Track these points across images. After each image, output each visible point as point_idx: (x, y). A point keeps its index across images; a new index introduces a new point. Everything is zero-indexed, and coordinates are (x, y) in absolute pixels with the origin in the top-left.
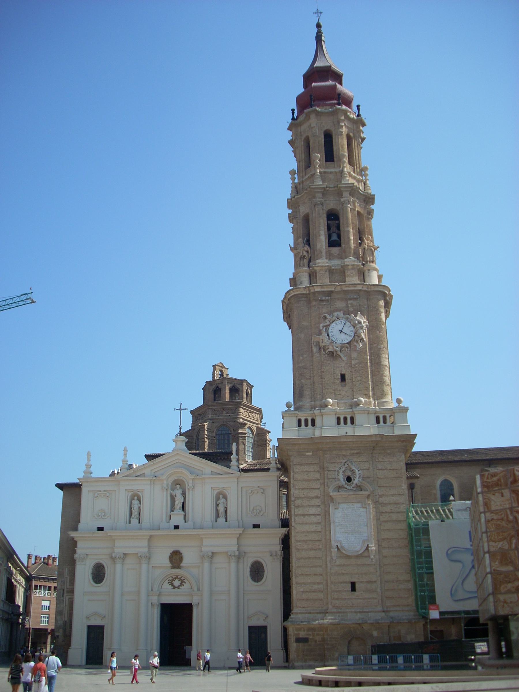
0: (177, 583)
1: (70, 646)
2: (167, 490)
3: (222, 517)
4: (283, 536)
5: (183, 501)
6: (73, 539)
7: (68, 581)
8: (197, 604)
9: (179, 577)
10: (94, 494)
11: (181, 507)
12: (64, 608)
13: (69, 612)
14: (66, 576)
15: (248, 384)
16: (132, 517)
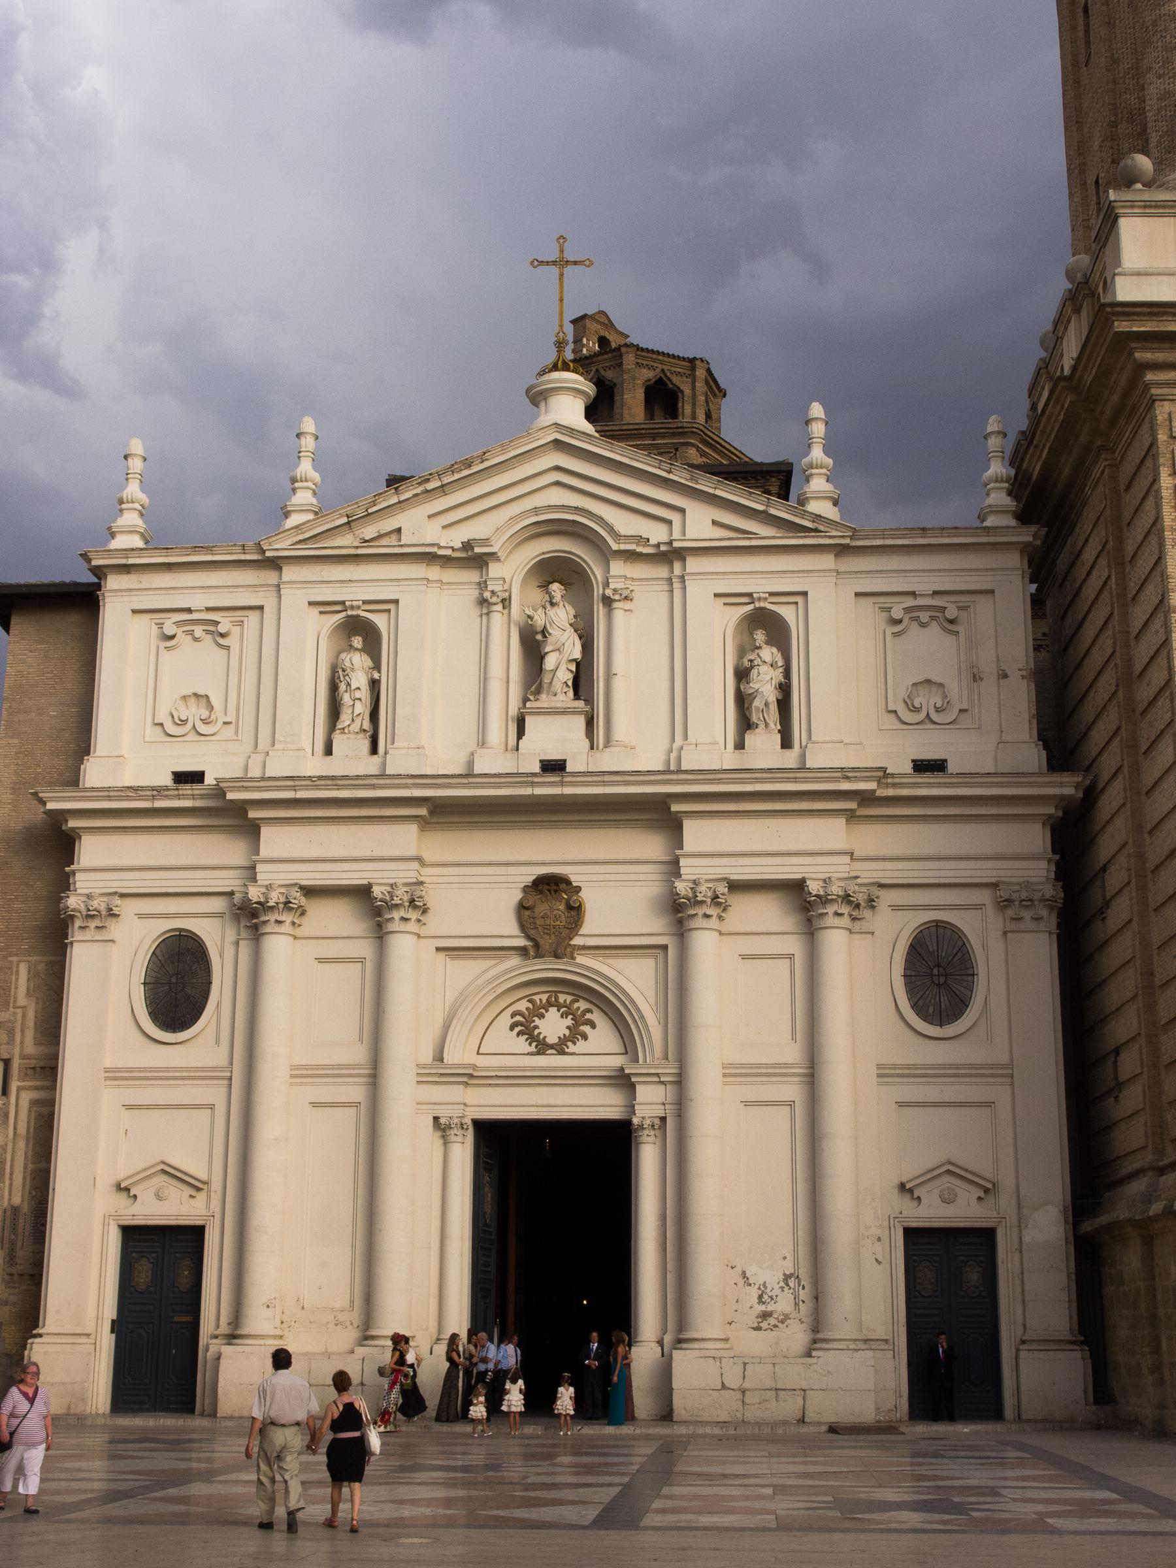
0: (553, 1026)
1: (36, 1326)
2: (506, 602)
3: (767, 725)
4: (1060, 814)
5: (577, 654)
6: (59, 817)
7: (30, 1023)
8: (657, 1122)
9: (562, 998)
10: (160, 626)
11: (570, 683)
12: (10, 1146)
13: (30, 1167)
14: (19, 1004)
15: (709, 379)
16: (339, 725)
